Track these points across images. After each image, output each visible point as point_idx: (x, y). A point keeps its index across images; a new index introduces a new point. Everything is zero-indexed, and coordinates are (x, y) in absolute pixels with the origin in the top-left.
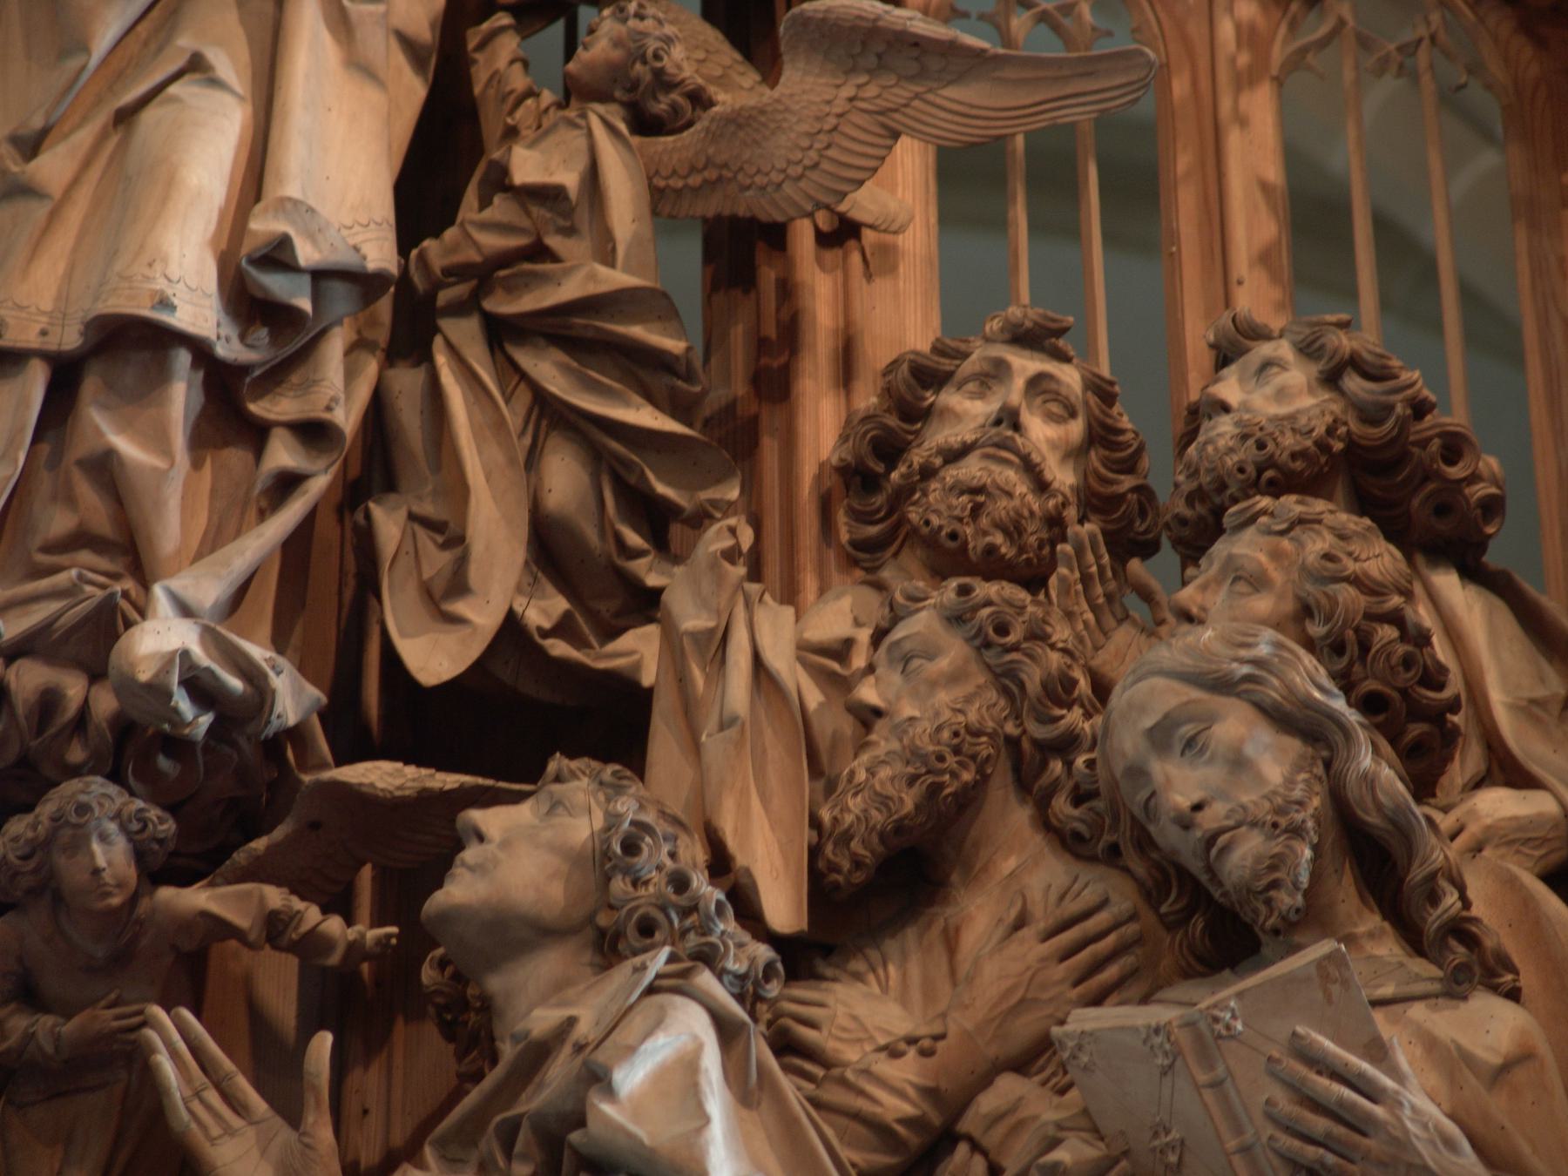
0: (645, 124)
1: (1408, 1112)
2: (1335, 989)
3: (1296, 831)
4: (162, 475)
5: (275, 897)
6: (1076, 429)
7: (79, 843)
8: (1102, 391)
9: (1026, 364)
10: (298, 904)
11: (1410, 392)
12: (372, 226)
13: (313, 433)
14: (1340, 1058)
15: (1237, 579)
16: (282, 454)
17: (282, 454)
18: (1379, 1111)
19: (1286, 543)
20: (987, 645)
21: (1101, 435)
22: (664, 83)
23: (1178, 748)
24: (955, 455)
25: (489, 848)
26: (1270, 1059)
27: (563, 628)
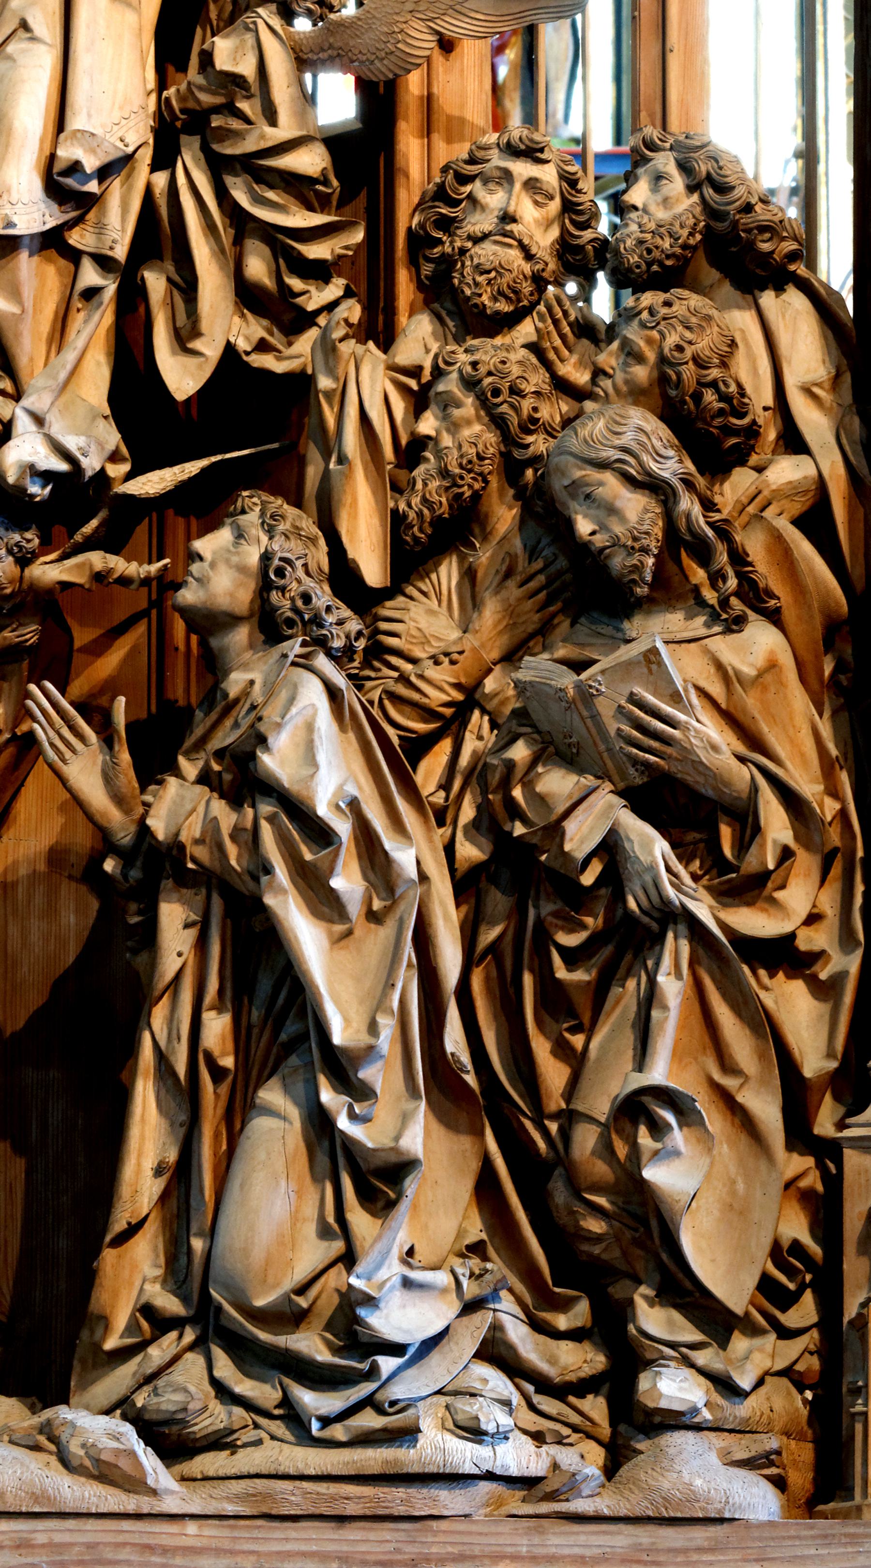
1: (692, 733)
2: (654, 667)
3: (645, 550)
4: (19, 318)
6: (555, 206)
8: (570, 181)
9: (522, 169)
12: (133, 115)
13: (104, 262)
14: (656, 706)
18: (676, 733)
19: (655, 334)
21: (569, 207)
23: (582, 497)
24: (477, 240)
25: (206, 565)
26: (620, 706)
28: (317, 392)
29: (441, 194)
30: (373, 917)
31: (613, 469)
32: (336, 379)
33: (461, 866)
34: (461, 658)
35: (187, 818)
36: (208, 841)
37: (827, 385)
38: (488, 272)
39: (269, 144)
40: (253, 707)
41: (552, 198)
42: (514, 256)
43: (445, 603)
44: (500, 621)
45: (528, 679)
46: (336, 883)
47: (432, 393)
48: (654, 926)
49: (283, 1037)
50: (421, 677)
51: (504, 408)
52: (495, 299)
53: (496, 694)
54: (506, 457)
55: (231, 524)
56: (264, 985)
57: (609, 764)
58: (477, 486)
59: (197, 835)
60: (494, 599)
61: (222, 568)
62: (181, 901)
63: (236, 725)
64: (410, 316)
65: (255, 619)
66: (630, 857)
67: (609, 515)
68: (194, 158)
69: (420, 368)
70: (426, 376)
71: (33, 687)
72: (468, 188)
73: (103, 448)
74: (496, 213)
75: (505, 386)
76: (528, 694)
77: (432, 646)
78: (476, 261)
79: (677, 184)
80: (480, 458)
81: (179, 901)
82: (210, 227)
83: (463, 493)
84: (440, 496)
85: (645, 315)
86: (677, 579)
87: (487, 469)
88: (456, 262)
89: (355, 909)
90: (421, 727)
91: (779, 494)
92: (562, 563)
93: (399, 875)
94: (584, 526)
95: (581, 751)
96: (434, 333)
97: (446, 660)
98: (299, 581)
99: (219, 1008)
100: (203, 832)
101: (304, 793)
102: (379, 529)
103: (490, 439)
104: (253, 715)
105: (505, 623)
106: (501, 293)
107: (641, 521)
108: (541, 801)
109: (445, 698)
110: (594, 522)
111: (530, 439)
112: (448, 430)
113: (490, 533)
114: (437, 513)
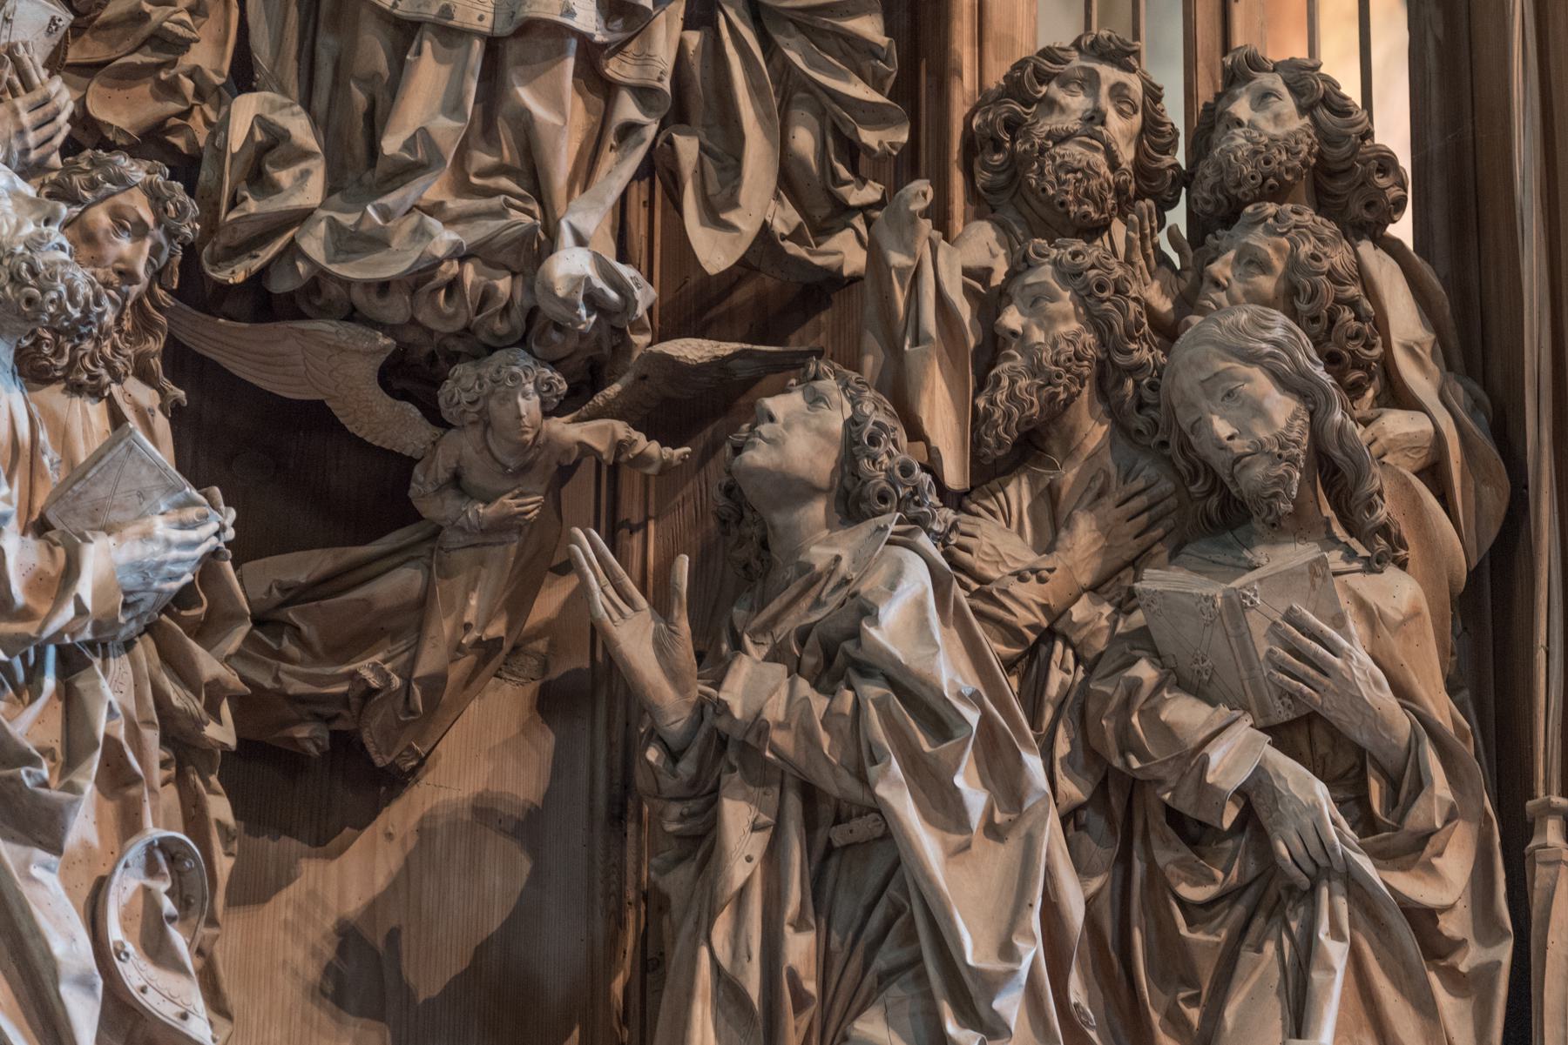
1: (1355, 663)
2: (1318, 581)
3: (1292, 461)
4: (558, 130)
5: (621, 429)
6: (1137, 119)
7: (509, 397)
9: (1109, 74)
10: (636, 435)
11: (1359, 127)
14: (1318, 626)
15: (1250, 262)
16: (628, 110)
17: (628, 110)
18: (1338, 662)
19: (1285, 242)
20: (1090, 295)
23: (1220, 395)
24: (1062, 138)
25: (778, 426)
26: (1275, 623)
27: (796, 236)
28: (889, 268)
29: (1015, 87)
30: (993, 831)
31: (1262, 365)
32: (912, 255)
33: (1064, 804)
34: (1051, 576)
35: (770, 696)
36: (793, 725)
37: (1428, 349)
38: (1075, 171)
40: (846, 581)
41: (1135, 112)
42: (1099, 159)
44: (1095, 541)
45: (1159, 589)
46: (959, 781)
47: (1015, 289)
48: (1305, 883)
49: (881, 963)
50: (1006, 592)
51: (1108, 305)
52: (1080, 203)
53: (1087, 624)
55: (803, 389)
56: (846, 907)
57: (1250, 696)
58: (1074, 389)
59: (781, 717)
60: (1088, 516)
61: (799, 430)
62: (747, 798)
63: (818, 603)
64: (965, 224)
65: (833, 494)
66: (1282, 796)
67: (1254, 417)
68: (738, 14)
69: (989, 271)
70: (998, 279)
71: (578, 531)
72: (1044, 89)
74: (1079, 114)
76: (1155, 607)
77: (1008, 566)
78: (1058, 160)
79: (1287, 104)
80: (1079, 357)
81: (744, 799)
82: (756, 89)
83: (1058, 394)
84: (1031, 395)
85: (1270, 221)
86: (1311, 506)
87: (1086, 372)
88: (1032, 164)
89: (976, 816)
91: (1393, 445)
92: (1166, 486)
93: (1030, 783)
94: (1222, 428)
95: (1215, 679)
96: (998, 240)
97: (1034, 578)
98: (890, 455)
99: (800, 925)
100: (787, 714)
101: (926, 671)
102: (956, 429)
104: (843, 592)
105: (1100, 544)
106: (1087, 194)
107: (1290, 427)
108: (1167, 732)
109: (1032, 619)
110: (1232, 426)
111: (1133, 346)
112: (1040, 326)
113: (1078, 448)
114: (1027, 413)
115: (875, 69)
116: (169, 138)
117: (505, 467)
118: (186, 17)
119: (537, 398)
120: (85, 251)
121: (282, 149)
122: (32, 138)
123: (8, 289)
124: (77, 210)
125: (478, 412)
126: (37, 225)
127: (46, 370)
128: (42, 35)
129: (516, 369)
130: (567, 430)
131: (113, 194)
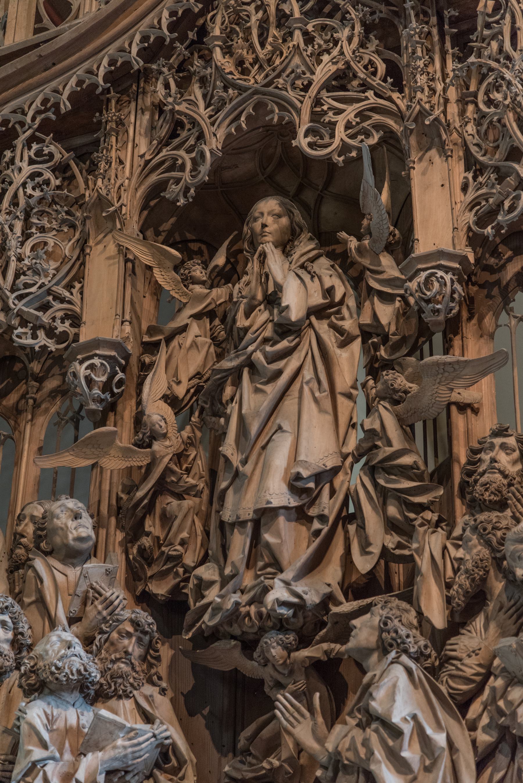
0: (396, 402)
4: (281, 545)
5: (325, 646)
9: (498, 441)
16: (316, 525)
17: (316, 525)
22: (396, 391)
27: (400, 546)
39: (388, 454)
43: (479, 634)
54: (494, 558)
72: (478, 456)
73: (319, 593)
75: (489, 527)
90: (464, 687)
102: (442, 604)
103: (486, 552)
115: (414, 473)
116: (184, 591)
117: (284, 674)
118: (179, 548)
119: (279, 647)
120: (112, 649)
121: (203, 584)
122: (105, 613)
123: (50, 677)
124: (106, 636)
125: (263, 659)
126: (66, 650)
127: (107, 694)
128: (105, 576)
129: (265, 640)
130: (305, 653)
131: (118, 626)
